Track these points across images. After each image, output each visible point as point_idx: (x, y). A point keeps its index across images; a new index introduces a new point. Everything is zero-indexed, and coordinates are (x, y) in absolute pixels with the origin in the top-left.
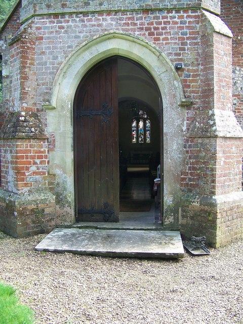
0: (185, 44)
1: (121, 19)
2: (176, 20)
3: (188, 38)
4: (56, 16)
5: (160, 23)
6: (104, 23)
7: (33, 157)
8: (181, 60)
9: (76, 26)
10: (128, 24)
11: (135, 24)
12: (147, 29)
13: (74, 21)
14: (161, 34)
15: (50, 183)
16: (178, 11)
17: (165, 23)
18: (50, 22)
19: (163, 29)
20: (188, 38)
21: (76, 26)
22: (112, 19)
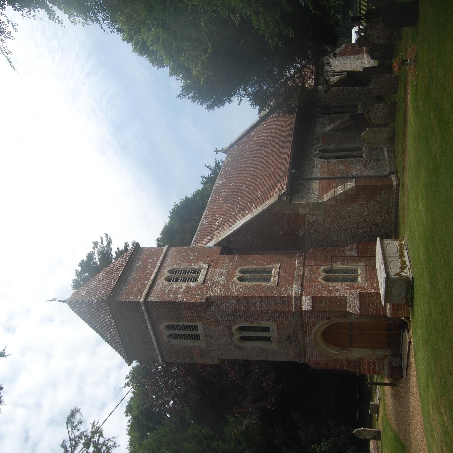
0: (317, 316)
1: (306, 335)
2: (306, 318)
3: (314, 314)
4: (305, 355)
5: (308, 324)
6: (308, 341)
7: (368, 367)
8: (324, 317)
9: (309, 349)
10: (309, 334)
11: (309, 331)
12: (311, 327)
13: (307, 350)
14: (313, 323)
15: (380, 360)
16: (303, 317)
17: (308, 321)
18: (307, 357)
19: (310, 322)
20: (314, 314)
21: (309, 349)
22: (307, 338)
